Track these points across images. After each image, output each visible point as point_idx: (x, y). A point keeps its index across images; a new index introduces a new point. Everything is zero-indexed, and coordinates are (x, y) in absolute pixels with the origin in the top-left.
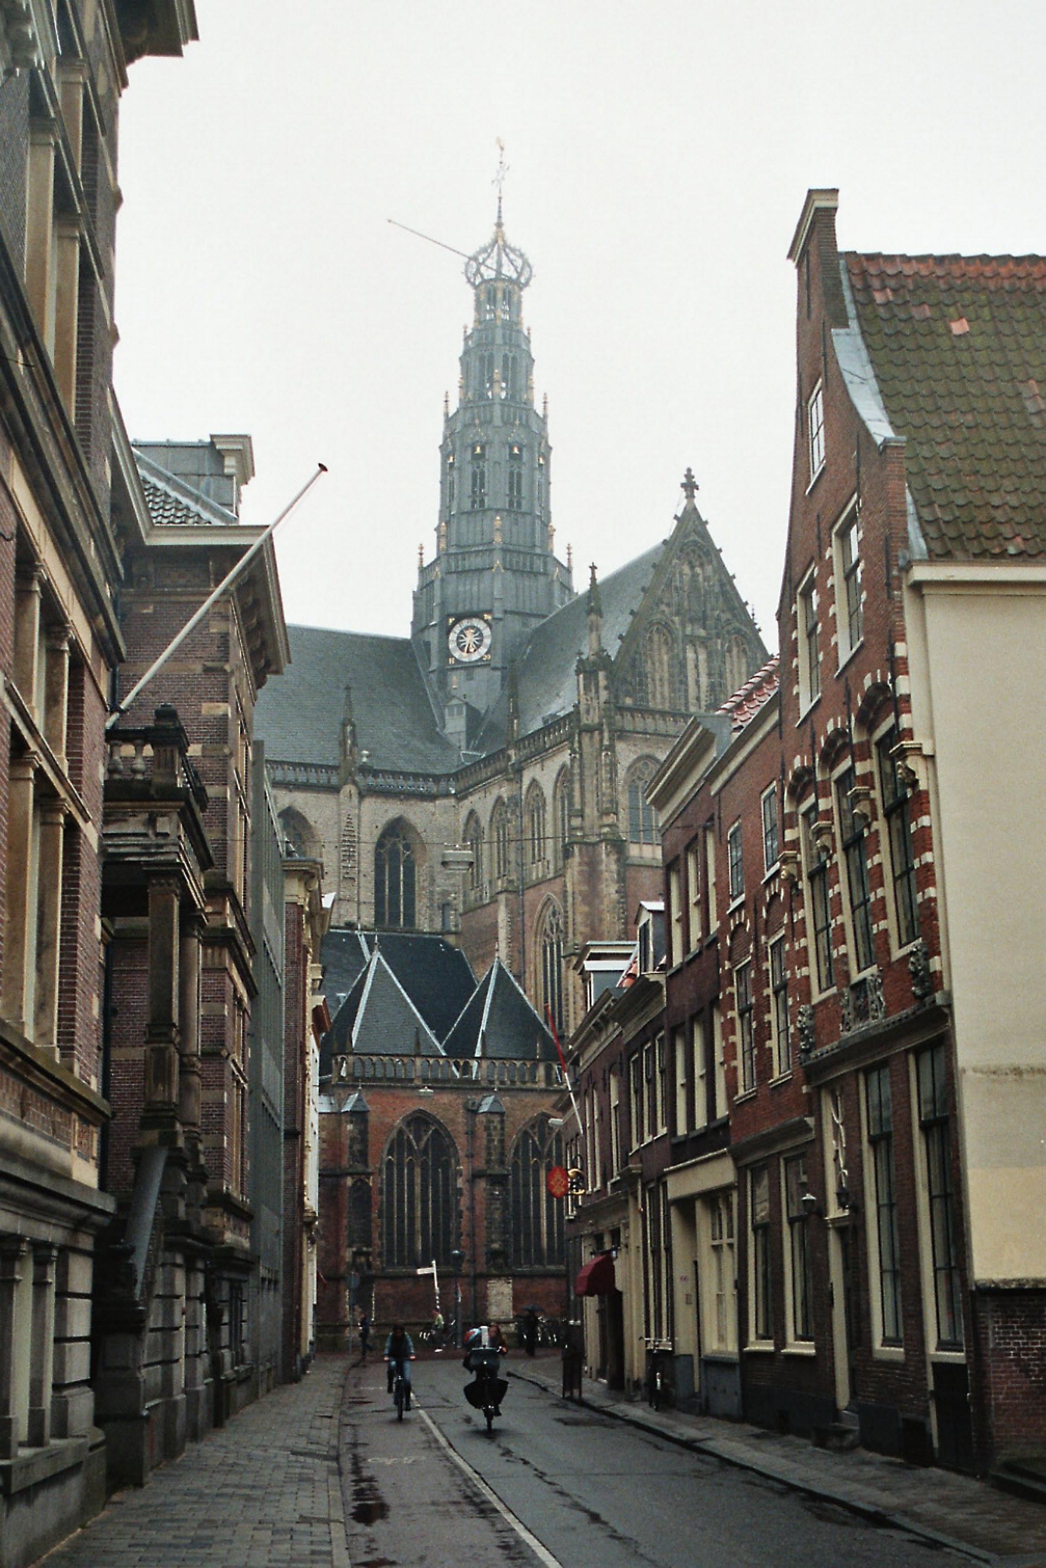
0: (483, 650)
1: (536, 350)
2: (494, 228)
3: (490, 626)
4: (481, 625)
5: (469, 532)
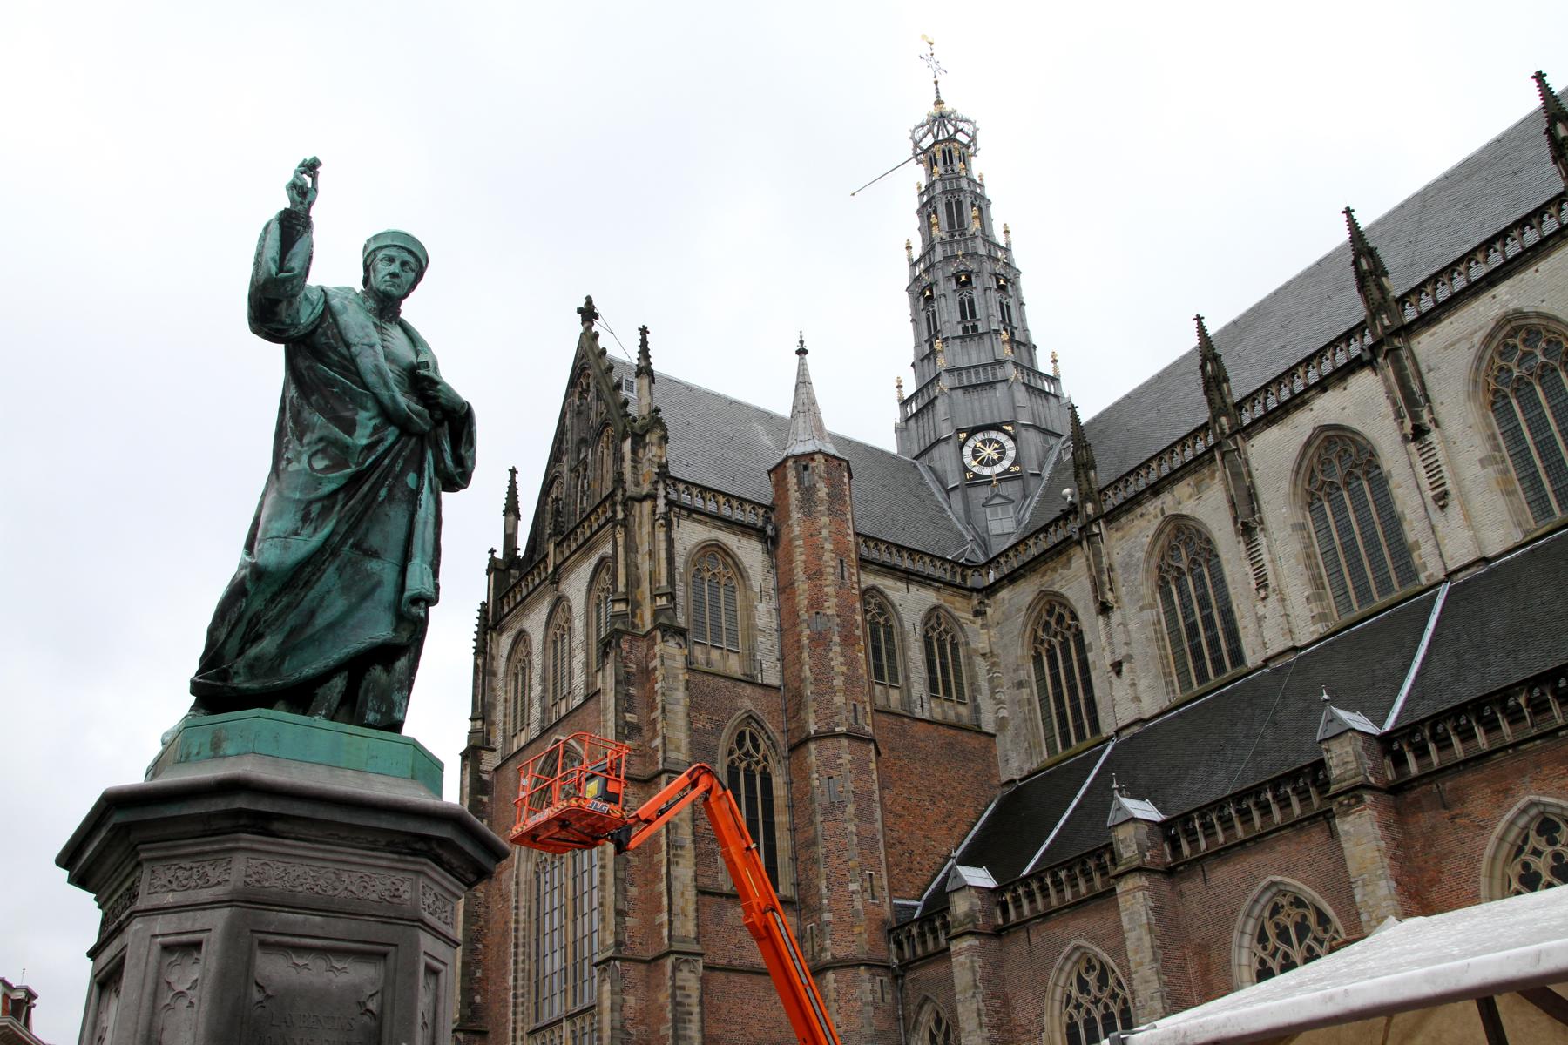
0: (1006, 463)
3: (1014, 438)
4: (1002, 437)
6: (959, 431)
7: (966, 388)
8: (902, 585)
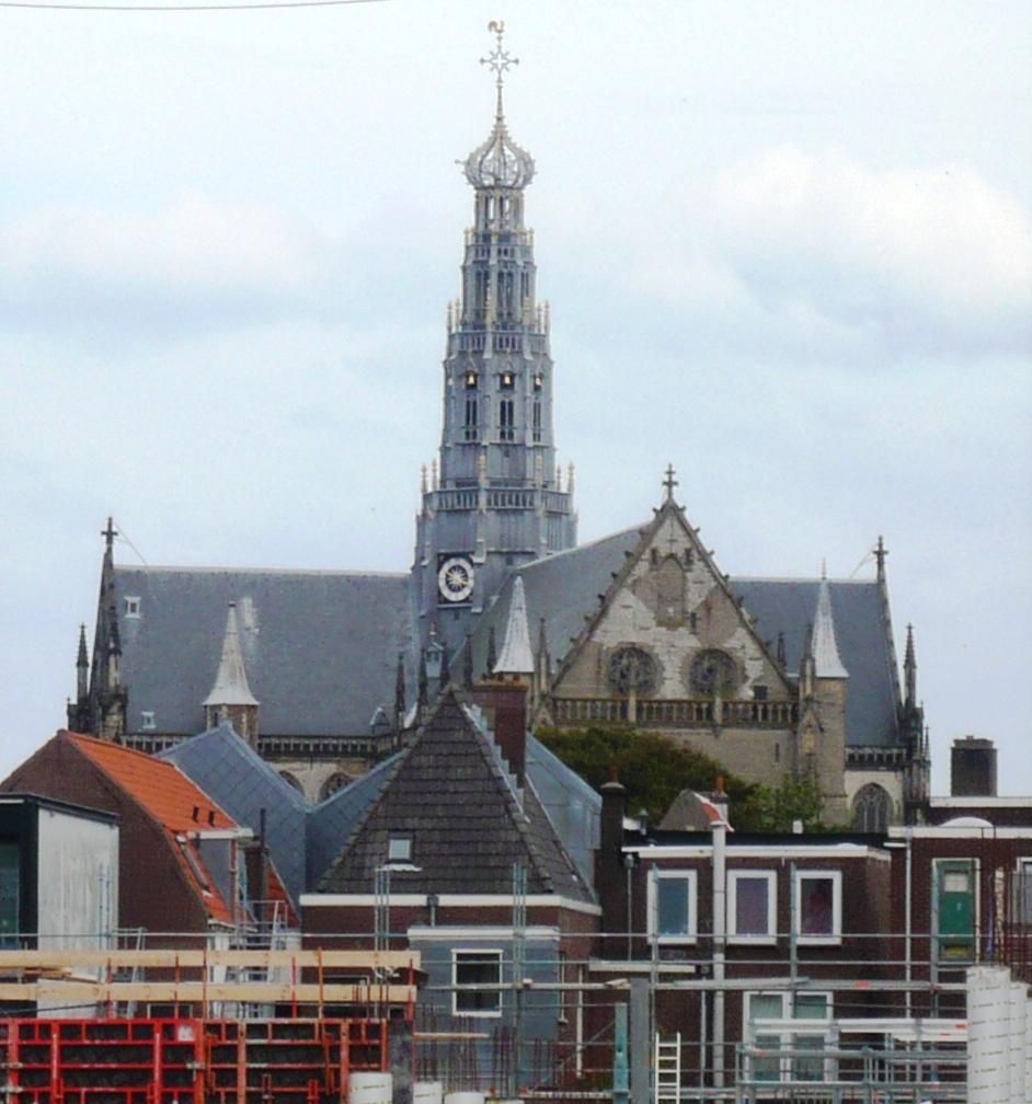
1: (538, 256)
2: (495, 121)
5: (460, 469)
6: (439, 555)
7: (449, 512)
8: (308, 765)
